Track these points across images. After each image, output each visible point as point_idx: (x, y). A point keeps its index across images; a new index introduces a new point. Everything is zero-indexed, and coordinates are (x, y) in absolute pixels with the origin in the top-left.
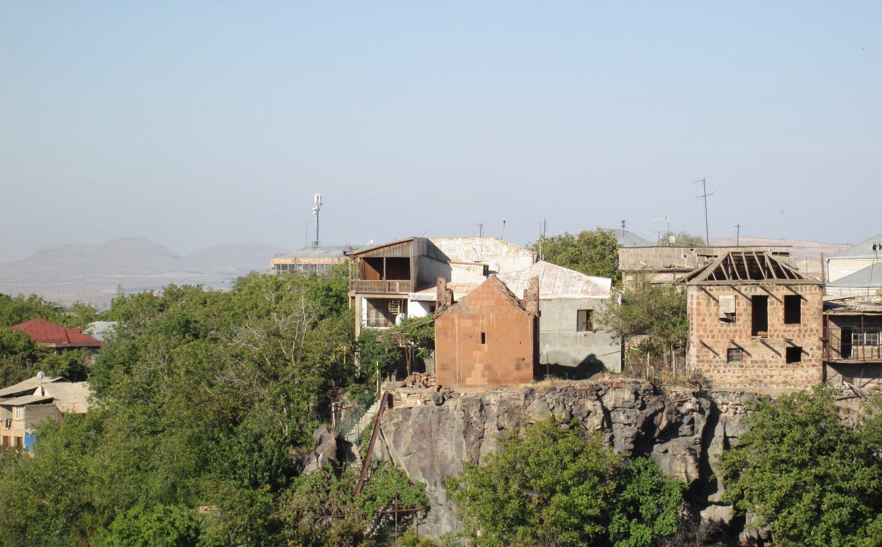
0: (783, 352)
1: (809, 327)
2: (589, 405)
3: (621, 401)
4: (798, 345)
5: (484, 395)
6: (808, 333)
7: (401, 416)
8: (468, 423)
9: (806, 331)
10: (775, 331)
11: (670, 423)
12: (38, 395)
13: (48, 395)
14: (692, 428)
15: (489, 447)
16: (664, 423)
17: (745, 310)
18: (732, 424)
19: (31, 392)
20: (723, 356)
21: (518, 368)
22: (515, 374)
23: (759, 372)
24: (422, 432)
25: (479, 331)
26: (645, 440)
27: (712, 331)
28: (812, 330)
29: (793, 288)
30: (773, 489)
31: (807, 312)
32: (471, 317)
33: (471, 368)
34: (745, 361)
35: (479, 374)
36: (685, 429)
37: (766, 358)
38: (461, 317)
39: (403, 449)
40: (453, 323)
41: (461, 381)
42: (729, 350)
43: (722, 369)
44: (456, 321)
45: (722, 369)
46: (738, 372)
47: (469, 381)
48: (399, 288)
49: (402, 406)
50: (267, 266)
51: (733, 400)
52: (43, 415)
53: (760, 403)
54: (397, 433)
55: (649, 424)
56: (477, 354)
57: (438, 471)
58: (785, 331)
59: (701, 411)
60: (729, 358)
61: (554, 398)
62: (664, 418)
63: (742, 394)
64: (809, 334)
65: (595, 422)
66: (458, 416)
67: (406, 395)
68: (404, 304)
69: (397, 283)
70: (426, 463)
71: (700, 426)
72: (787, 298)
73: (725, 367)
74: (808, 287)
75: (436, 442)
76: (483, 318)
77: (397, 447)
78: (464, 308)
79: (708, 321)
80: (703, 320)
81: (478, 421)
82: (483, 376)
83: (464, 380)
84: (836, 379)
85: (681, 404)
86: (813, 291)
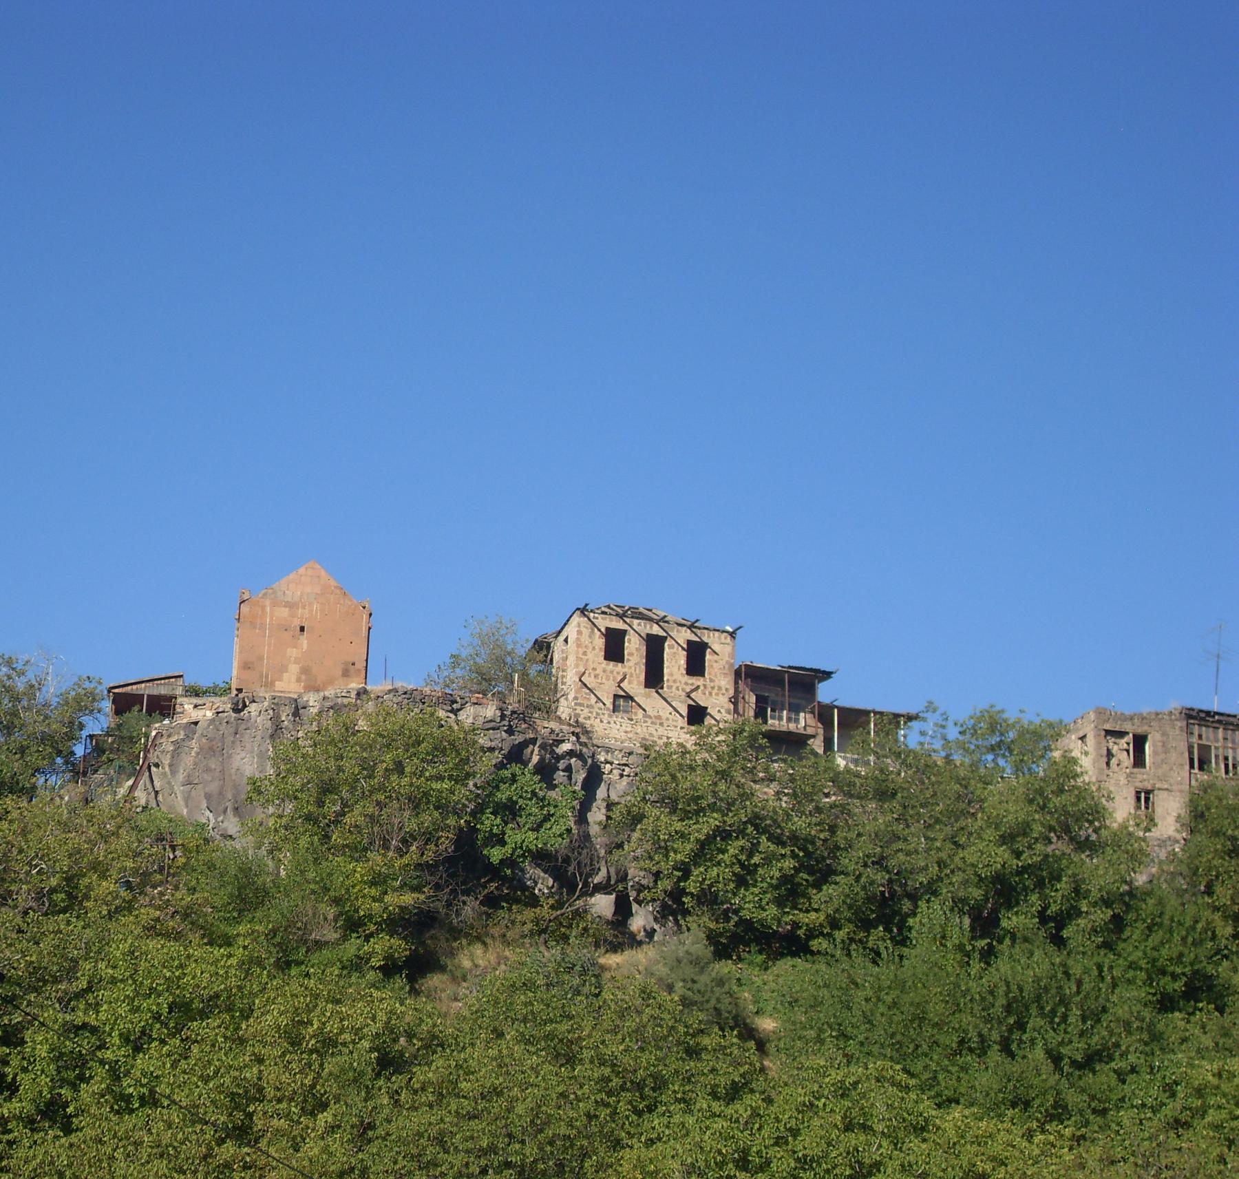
0: (684, 712)
1: (716, 683)
3: (481, 720)
4: (702, 704)
5: (300, 696)
6: (715, 691)
7: (182, 733)
8: (277, 729)
9: (713, 688)
10: (675, 681)
11: (542, 760)
14: (570, 778)
16: (535, 759)
17: (637, 649)
18: (617, 786)
20: (609, 703)
21: (346, 674)
23: (652, 730)
24: (211, 748)
25: (297, 623)
27: (594, 669)
28: (720, 688)
29: (698, 632)
31: (715, 665)
32: (289, 605)
33: (284, 669)
34: (636, 714)
35: (294, 679)
37: (661, 713)
38: (275, 604)
39: (181, 776)
40: (263, 608)
42: (616, 697)
43: (605, 718)
44: (268, 609)
45: (605, 718)
46: (627, 725)
47: (279, 685)
49: (185, 721)
51: (618, 758)
56: (292, 652)
57: (230, 796)
58: (686, 684)
59: (580, 756)
60: (615, 709)
61: (395, 700)
62: (536, 752)
63: (630, 754)
64: (716, 691)
67: (191, 706)
70: (213, 787)
71: (580, 776)
72: (689, 642)
73: (610, 716)
74: (717, 634)
75: (230, 756)
76: (304, 607)
77: (173, 772)
78: (279, 593)
79: (590, 656)
80: (585, 653)
81: (291, 727)
82: (299, 680)
83: (273, 684)
85: (559, 742)
86: (723, 640)
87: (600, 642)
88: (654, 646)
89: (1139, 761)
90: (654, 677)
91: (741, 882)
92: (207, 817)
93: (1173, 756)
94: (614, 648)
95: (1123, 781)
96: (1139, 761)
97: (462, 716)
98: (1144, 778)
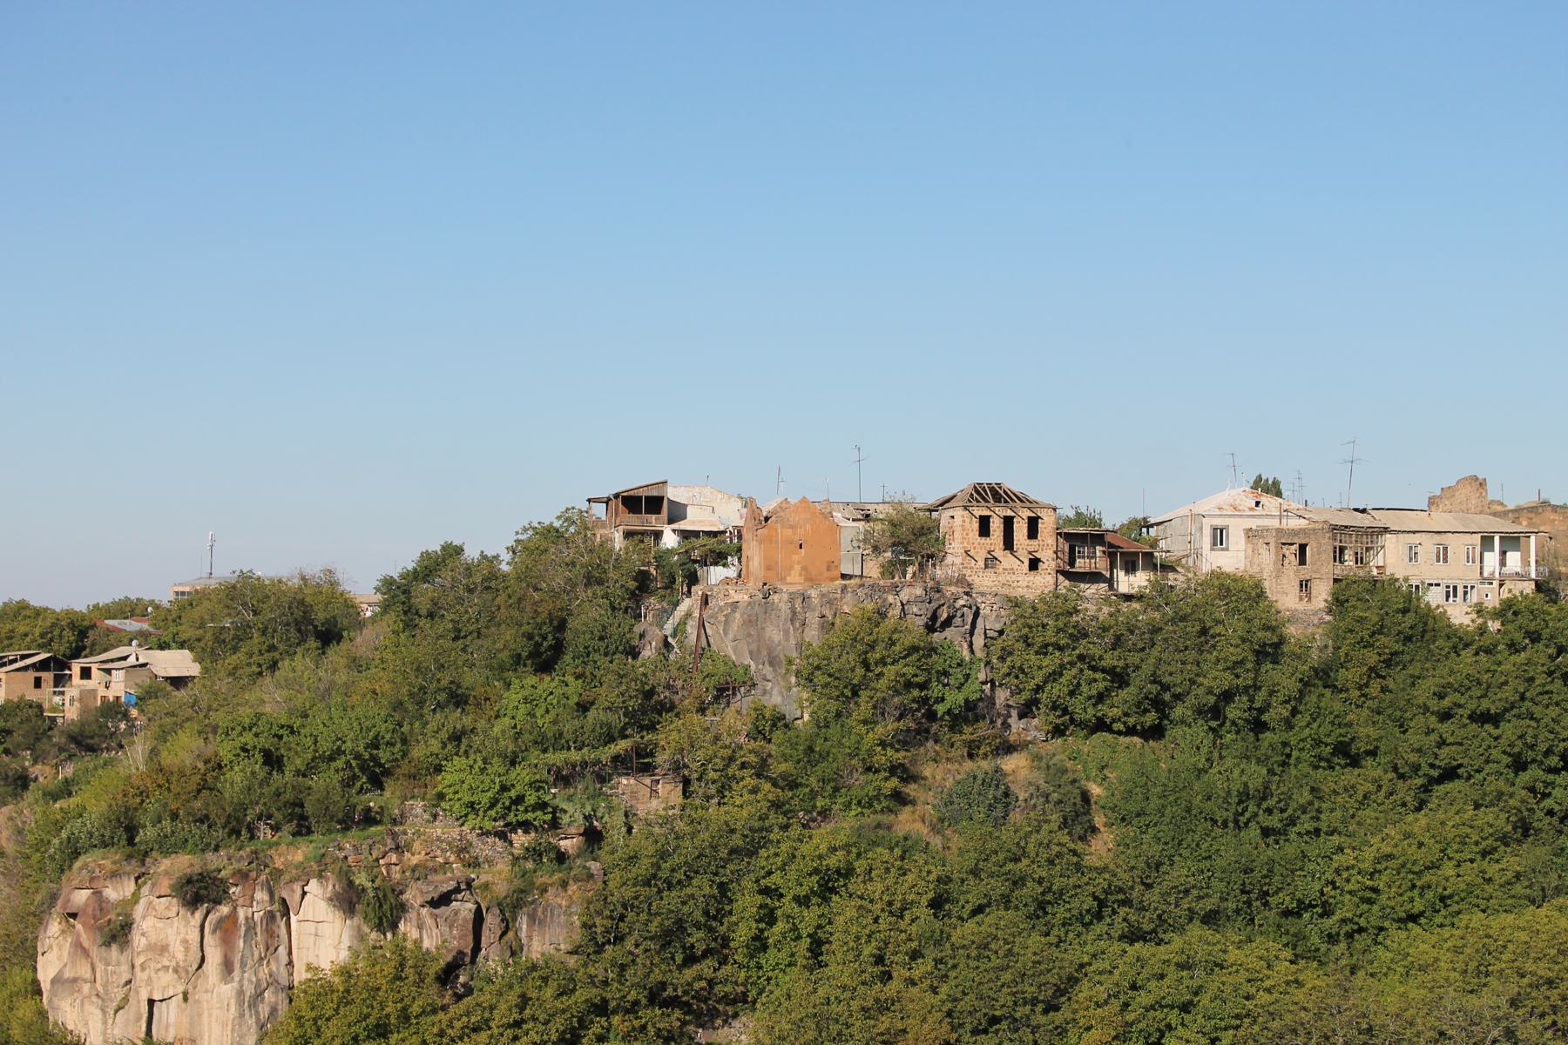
2: (891, 598)
8: (794, 613)
12: (132, 661)
13: (142, 661)
15: (813, 634)
16: (945, 616)
18: (991, 620)
19: (125, 658)
20: (981, 564)
22: (827, 574)
26: (930, 628)
30: (1040, 668)
32: (792, 527)
33: (791, 568)
36: (957, 621)
39: (731, 636)
41: (783, 579)
46: (993, 577)
47: (789, 579)
48: (653, 521)
50: (147, 597)
52: (143, 678)
53: (1016, 603)
54: (726, 623)
55: (934, 617)
56: (796, 557)
60: (986, 566)
64: (1047, 547)
65: (897, 611)
66: (784, 608)
68: (658, 535)
69: (654, 516)
70: (754, 646)
84: (1065, 583)
87: (976, 525)
88: (1008, 522)
89: (1302, 562)
90: (1009, 544)
91: (1072, 693)
92: (747, 661)
93: (1324, 556)
94: (984, 527)
95: (1292, 575)
96: (1302, 562)
97: (902, 594)
98: (1305, 573)
